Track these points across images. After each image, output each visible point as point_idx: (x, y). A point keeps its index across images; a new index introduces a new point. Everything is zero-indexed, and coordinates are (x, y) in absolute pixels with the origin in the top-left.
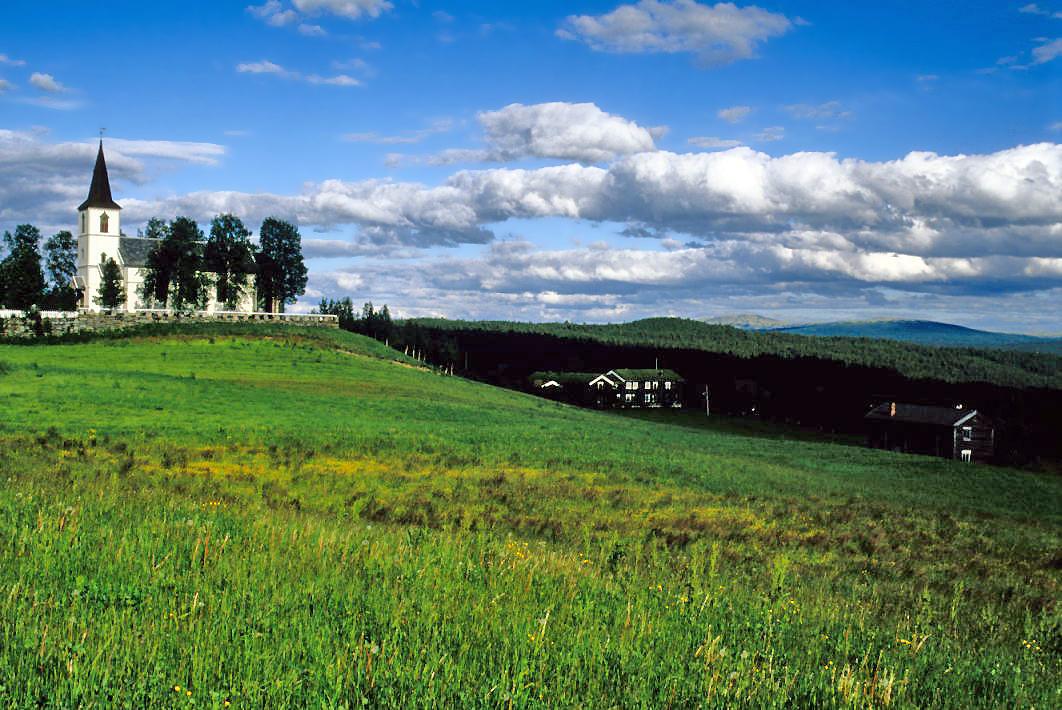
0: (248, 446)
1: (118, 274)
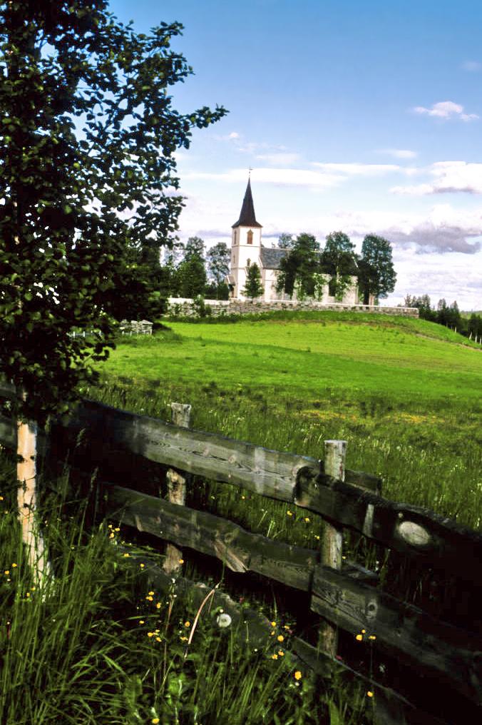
0: (346, 401)
1: (258, 274)
